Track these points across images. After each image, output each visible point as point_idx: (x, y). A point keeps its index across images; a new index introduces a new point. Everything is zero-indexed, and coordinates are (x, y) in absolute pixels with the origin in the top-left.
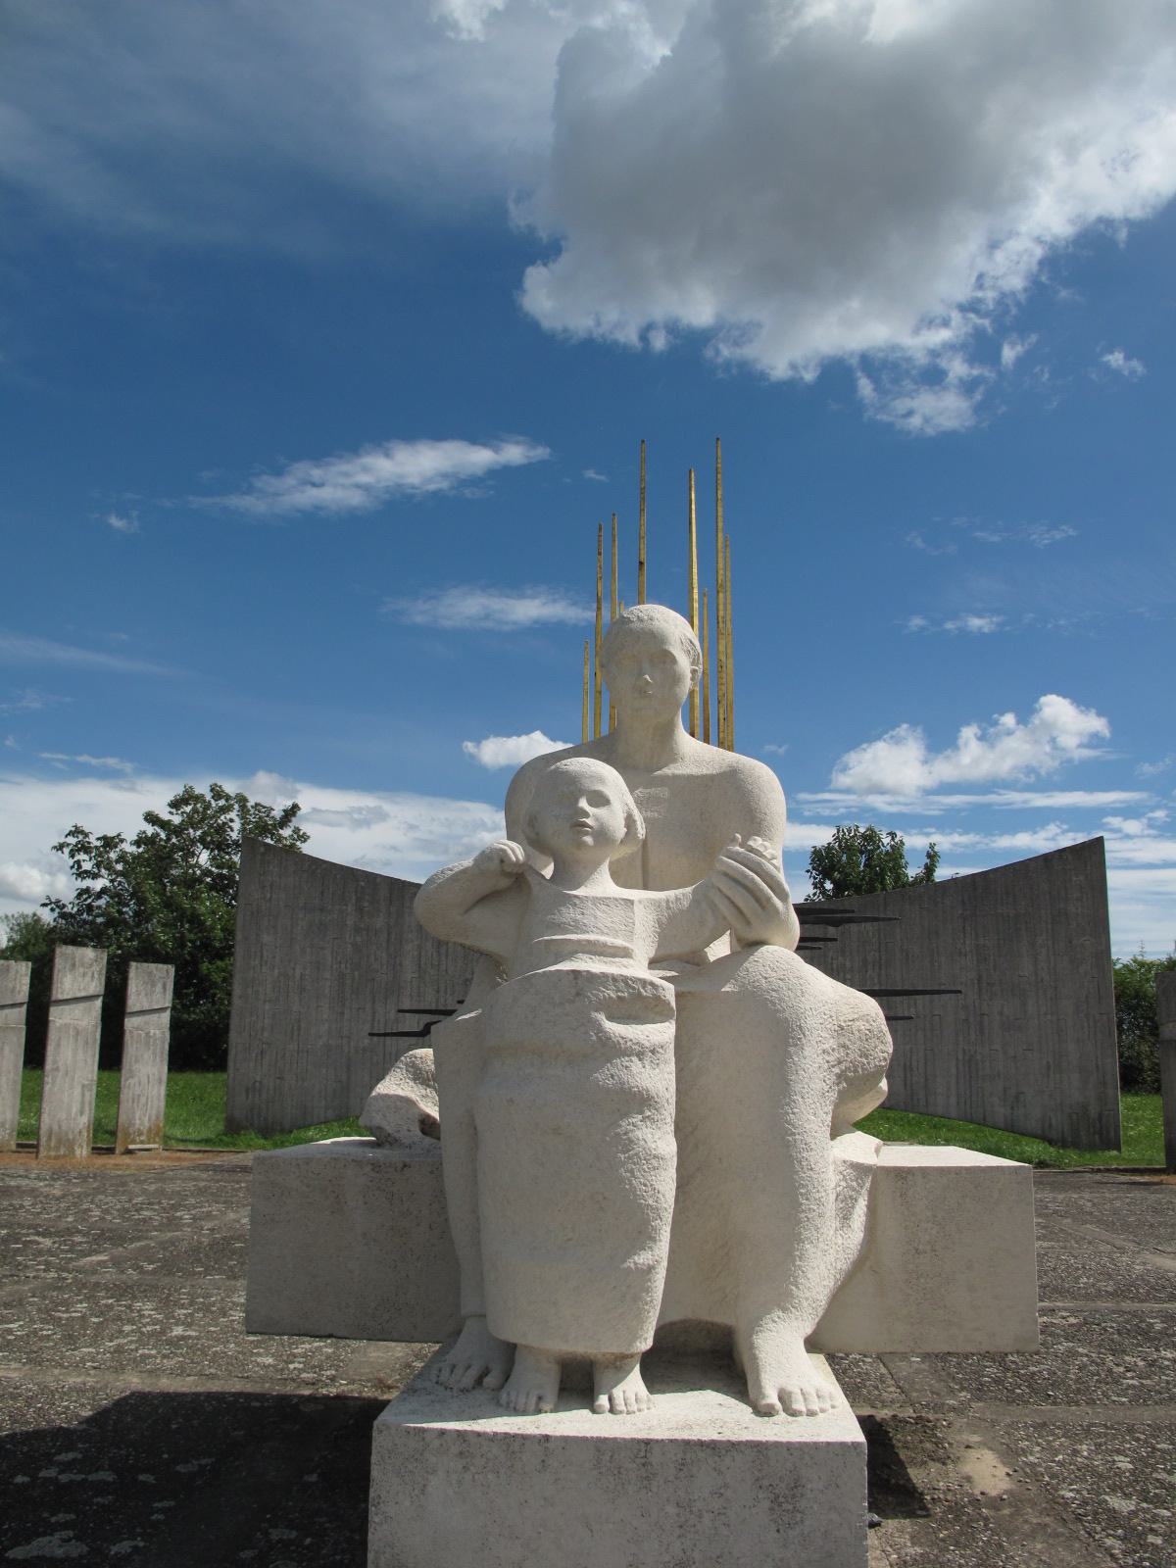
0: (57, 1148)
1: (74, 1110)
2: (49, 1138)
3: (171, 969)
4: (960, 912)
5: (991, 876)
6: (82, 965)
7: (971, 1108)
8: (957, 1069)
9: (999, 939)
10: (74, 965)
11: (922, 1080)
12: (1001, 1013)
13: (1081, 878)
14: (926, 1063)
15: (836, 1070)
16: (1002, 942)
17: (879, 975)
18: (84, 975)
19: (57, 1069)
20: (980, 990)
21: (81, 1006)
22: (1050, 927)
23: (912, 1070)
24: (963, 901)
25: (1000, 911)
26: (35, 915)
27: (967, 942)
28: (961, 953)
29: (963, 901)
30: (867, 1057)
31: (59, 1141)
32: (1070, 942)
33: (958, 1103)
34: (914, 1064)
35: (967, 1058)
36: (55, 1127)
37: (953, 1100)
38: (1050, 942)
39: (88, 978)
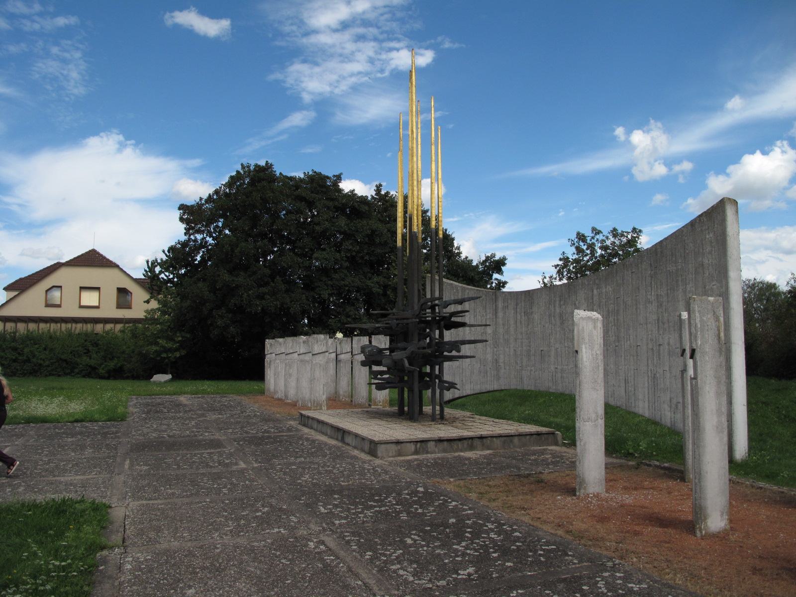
0: (316, 407)
1: (321, 393)
2: (314, 403)
3: (388, 337)
4: (650, 272)
5: (665, 243)
6: (320, 341)
7: (655, 410)
8: (648, 383)
9: (667, 290)
10: (317, 341)
11: (633, 389)
12: (669, 344)
13: (711, 235)
14: (634, 379)
16: (669, 291)
17: (614, 319)
18: (321, 345)
19: (315, 379)
20: (658, 328)
21: (321, 354)
22: (694, 276)
23: (628, 382)
24: (651, 264)
25: (668, 269)
26: (755, 279)
27: (653, 294)
28: (650, 301)
29: (651, 264)
31: (317, 404)
32: (705, 288)
33: (649, 406)
34: (630, 378)
35: (653, 375)
36: (316, 399)
37: (646, 405)
38: (693, 289)
39: (322, 346)
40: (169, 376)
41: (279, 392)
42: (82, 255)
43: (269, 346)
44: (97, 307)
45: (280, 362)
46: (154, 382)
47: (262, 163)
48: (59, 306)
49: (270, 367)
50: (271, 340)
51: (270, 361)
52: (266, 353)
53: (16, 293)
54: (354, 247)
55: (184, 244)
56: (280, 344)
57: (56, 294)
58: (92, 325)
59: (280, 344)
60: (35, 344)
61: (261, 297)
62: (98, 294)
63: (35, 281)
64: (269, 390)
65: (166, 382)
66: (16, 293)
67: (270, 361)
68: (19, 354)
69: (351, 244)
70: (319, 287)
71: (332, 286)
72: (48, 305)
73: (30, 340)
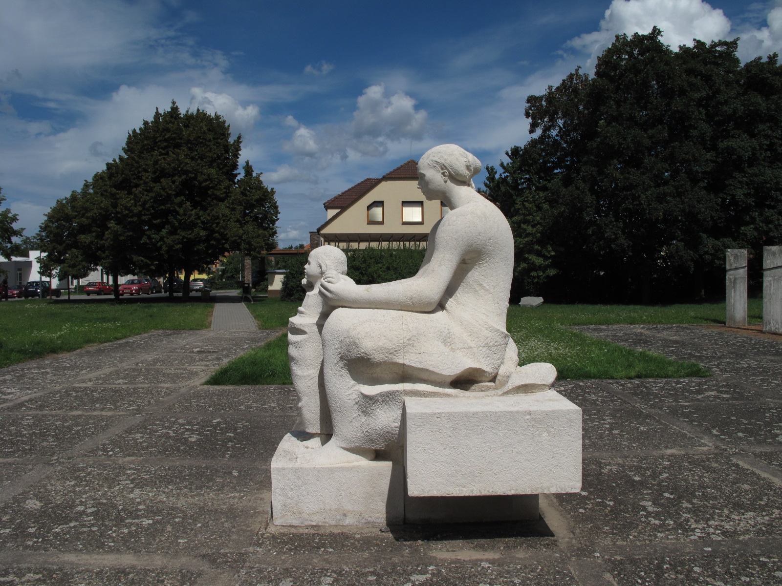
15: (340, 356)
30: (350, 352)
40: (540, 300)
41: (772, 322)
42: (402, 166)
43: (732, 258)
44: (421, 223)
45: (774, 280)
46: (525, 306)
47: (646, 31)
48: (382, 223)
49: (734, 287)
50: (736, 251)
51: (735, 279)
52: (728, 267)
53: (339, 210)
54: (773, 131)
55: (534, 143)
56: (774, 254)
57: (378, 211)
58: (398, 243)
59: (774, 254)
60: (379, 263)
61: (661, 199)
62: (421, 208)
63: (356, 197)
64: (733, 318)
65: (538, 306)
66: (339, 210)
67: (735, 279)
68: (362, 273)
69: (771, 128)
70: (731, 185)
71: (747, 184)
72: (371, 222)
73: (371, 258)
